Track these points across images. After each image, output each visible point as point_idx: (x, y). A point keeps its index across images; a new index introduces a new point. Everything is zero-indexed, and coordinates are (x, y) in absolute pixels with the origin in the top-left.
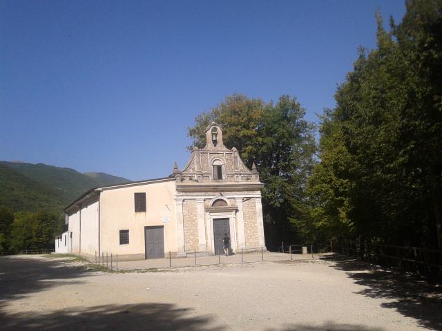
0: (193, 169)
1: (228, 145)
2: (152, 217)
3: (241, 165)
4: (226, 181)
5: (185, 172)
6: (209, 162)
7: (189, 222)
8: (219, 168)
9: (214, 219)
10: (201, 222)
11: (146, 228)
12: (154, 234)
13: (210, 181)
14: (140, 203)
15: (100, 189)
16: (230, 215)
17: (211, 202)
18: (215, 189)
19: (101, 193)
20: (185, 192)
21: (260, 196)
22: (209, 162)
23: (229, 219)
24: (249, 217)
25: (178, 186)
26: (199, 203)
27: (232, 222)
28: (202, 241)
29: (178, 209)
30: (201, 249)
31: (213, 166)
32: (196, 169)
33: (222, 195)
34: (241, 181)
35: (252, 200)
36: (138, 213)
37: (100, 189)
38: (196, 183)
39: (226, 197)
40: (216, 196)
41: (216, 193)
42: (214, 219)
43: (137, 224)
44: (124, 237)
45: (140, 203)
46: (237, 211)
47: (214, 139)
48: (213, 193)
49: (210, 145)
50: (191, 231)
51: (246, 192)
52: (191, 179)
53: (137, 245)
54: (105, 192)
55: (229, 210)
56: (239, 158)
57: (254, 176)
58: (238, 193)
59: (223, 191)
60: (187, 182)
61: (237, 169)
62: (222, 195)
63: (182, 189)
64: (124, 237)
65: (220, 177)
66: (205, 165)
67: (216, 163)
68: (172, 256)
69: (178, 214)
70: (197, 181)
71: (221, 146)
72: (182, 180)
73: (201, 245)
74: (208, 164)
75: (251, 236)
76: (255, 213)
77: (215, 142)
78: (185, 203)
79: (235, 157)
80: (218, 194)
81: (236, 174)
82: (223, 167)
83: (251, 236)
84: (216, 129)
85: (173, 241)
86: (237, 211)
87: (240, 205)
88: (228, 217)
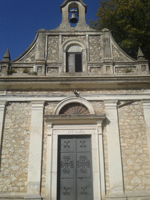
3: (115, 51)
5: (18, 62)
6: (61, 47)
8: (78, 57)
9: (60, 137)
10: (35, 141)
13: (60, 72)
16: (93, 130)
17: (53, 109)
18: (65, 85)
20: (13, 90)
22: (61, 47)
23: (89, 136)
28: (33, 176)
31: (68, 54)
32: (37, 58)
33: (77, 95)
35: (136, 106)
40: (68, 98)
41: (67, 93)
42: (60, 137)
46: (105, 122)
47: (73, 16)
48: (61, 93)
49: (65, 26)
50: (15, 157)
51: (125, 92)
52: (25, 72)
55: (91, 120)
56: (112, 42)
57: (139, 67)
58: (108, 92)
59: (81, 90)
65: (79, 68)
66: (54, 51)
67: (72, 49)
71: (82, 26)
72: (10, 73)
73: (30, 183)
74: (58, 50)
75: (136, 172)
77: (74, 21)
78: (9, 108)
79: (105, 40)
80: (71, 93)
81: (107, 63)
82: (84, 54)
83: (136, 172)
84: (76, 7)
86: (105, 122)
87: (112, 113)
88: (87, 132)
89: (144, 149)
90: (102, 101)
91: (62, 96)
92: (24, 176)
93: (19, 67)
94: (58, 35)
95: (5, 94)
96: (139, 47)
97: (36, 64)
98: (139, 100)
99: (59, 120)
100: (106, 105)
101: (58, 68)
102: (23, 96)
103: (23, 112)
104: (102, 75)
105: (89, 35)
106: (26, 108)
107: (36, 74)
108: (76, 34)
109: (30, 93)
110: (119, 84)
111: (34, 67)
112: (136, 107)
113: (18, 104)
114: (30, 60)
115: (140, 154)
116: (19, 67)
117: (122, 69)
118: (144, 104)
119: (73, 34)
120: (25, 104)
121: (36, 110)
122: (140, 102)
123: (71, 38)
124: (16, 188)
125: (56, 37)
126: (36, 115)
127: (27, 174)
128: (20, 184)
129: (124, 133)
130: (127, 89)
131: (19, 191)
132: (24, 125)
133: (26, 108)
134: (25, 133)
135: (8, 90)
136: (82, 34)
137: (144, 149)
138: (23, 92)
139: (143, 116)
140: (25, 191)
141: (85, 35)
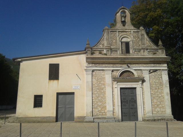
0: (103, 45)
1: (137, 24)
2: (63, 84)
3: (147, 42)
4: (133, 54)
5: (95, 47)
6: (118, 38)
7: (97, 90)
8: (127, 44)
9: (121, 88)
10: (108, 91)
11: (58, 94)
12: (65, 99)
13: (118, 55)
14: (54, 73)
15: (20, 60)
16: (137, 85)
17: (117, 74)
18: (122, 62)
19: (21, 63)
20: (95, 64)
21: (166, 68)
22: (118, 38)
23: (135, 88)
24: (155, 88)
25: (87, 58)
27: (139, 92)
28: (109, 107)
29: (87, 78)
30: (109, 115)
31: (122, 42)
32: (105, 45)
33: (129, 67)
34: (147, 55)
35: (158, 73)
36: (52, 81)
37: (20, 60)
38: (105, 56)
39: (133, 68)
40: (124, 68)
41: (123, 66)
42: (121, 88)
43: (50, 90)
44: (38, 101)
45: (54, 73)
46: (143, 81)
47: (123, 19)
48: (120, 65)
49: (119, 25)
50: (99, 98)
51: (153, 65)
52: (100, 53)
53: (49, 109)
54: (23, 62)
55: (136, 80)
56: (146, 36)
57: (160, 51)
58: (145, 65)
59: (130, 64)
60: (97, 55)
61: (143, 44)
62: (129, 67)
63: (91, 61)
64: (38, 101)
65: (128, 51)
66: (114, 41)
67: (124, 40)
68: (82, 120)
69: (87, 82)
70: (106, 54)
71: (129, 26)
72: (92, 54)
73: (108, 111)
75: (158, 105)
76: (161, 84)
77: (124, 23)
78: (94, 73)
79: (142, 35)
80: (125, 66)
81: (144, 49)
82: (131, 43)
83: (158, 105)
84: (125, 12)
85: (82, 107)
86: (143, 81)
88: (134, 86)
89: (162, 94)
90: (141, 70)
91: (121, 67)
92: (105, 107)
93: (96, 50)
94: (116, 31)
95: (91, 66)
96: (160, 40)
97: (106, 49)
98: (160, 70)
99: (121, 80)
100: (143, 72)
101: (117, 51)
102: (101, 67)
103: (101, 75)
104: (141, 56)
105: (133, 32)
106: (103, 74)
107: (106, 54)
108: (126, 31)
109: (104, 65)
110: (150, 61)
111: (105, 50)
112: (159, 73)
113: (98, 71)
114: (102, 46)
115: (160, 97)
116: (96, 50)
117: (151, 52)
118: (162, 72)
119: (124, 31)
120: (102, 71)
121: (107, 74)
122: (160, 71)
123: (123, 33)
124: (101, 113)
125: (115, 32)
126: (108, 77)
127: (106, 106)
128: (103, 111)
129: (152, 87)
130: (154, 64)
131: (102, 115)
132: (102, 82)
133: (103, 74)
134: (103, 86)
135: (92, 64)
136: (130, 31)
137: (162, 94)
138: (100, 65)
139: (162, 78)
140: (106, 115)
141: (131, 32)
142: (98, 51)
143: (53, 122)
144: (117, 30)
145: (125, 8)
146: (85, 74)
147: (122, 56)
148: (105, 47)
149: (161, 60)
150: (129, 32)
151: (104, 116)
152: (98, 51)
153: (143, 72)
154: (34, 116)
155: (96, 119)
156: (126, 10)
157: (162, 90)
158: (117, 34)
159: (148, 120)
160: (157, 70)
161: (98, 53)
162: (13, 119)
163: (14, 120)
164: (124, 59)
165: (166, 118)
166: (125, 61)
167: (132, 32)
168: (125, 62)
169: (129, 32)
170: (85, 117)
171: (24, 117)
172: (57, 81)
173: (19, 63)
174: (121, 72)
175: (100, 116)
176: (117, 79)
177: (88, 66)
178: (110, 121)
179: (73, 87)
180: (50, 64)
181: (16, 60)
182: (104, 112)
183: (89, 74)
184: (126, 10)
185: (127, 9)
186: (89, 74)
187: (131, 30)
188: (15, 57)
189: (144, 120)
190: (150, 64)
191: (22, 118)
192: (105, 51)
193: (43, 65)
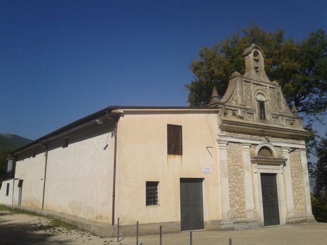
0: (236, 101)
1: (271, 76)
2: (191, 163)
4: (271, 122)
6: (253, 94)
7: (234, 174)
9: (262, 174)
11: (183, 180)
12: (191, 189)
13: (254, 119)
14: (175, 142)
15: (121, 111)
19: (121, 118)
21: (304, 147)
23: (275, 174)
24: (295, 176)
25: (224, 122)
26: (246, 148)
27: (280, 180)
28: (249, 205)
29: (221, 154)
30: (249, 217)
33: (269, 141)
34: (283, 124)
35: (297, 152)
36: (172, 156)
37: (121, 111)
38: (241, 121)
39: (274, 143)
42: (262, 174)
43: (170, 173)
44: (152, 192)
45: (175, 142)
50: (237, 190)
51: (292, 141)
52: (234, 114)
53: (169, 208)
54: (126, 116)
58: (284, 140)
60: (230, 117)
61: (281, 109)
62: (269, 141)
63: (228, 127)
64: (152, 192)
65: (262, 116)
66: (249, 97)
67: (260, 98)
68: (218, 226)
69: (222, 162)
70: (241, 118)
74: (251, 97)
76: (301, 169)
81: (282, 115)
85: (215, 206)
87: (286, 155)
88: (275, 172)
89: (302, 185)
90: (280, 147)
91: (260, 140)
92: (243, 204)
93: (229, 109)
94: (250, 82)
95: (225, 134)
97: (241, 108)
98: (298, 149)
99: (262, 161)
100: (283, 150)
101: (253, 114)
102: (237, 138)
103: (237, 152)
104: (280, 125)
105: (270, 87)
106: (238, 149)
107: (241, 118)
108: (262, 84)
109: (240, 135)
110: (291, 135)
111: (239, 111)
112: (297, 153)
113: (233, 144)
114: (235, 103)
115: (299, 188)
116: (229, 109)
117: (288, 121)
118: (302, 152)
119: (259, 83)
120: (237, 145)
121: (246, 151)
122: (298, 150)
123: (259, 87)
124: (239, 215)
125: (249, 83)
126: (246, 154)
127: (244, 203)
128: (242, 211)
130: (293, 139)
131: (241, 217)
132: (239, 163)
133: (238, 149)
134: (240, 170)
135: (226, 131)
136: (265, 84)
137: (302, 185)
138: (236, 134)
139: (300, 160)
140: (245, 217)
141: (266, 86)
142: (231, 110)
143: (178, 232)
144: (252, 81)
145: (259, 47)
146: (218, 147)
147: (260, 122)
148: (239, 104)
149: (301, 135)
150: (264, 86)
151: (244, 219)
152: (231, 110)
153: (283, 150)
154: (148, 223)
155: (240, 223)
156: (259, 52)
157: (302, 178)
158: (252, 87)
159: (292, 223)
160: (295, 149)
161: (231, 114)
162: (113, 229)
163: (113, 232)
164: (265, 128)
165: (308, 219)
166: (264, 131)
167: (268, 87)
168: (265, 133)
169: (264, 86)
170: (221, 221)
171: (131, 224)
172: (179, 156)
173: (117, 117)
174: (261, 147)
175: (239, 219)
176: (259, 160)
177: (221, 134)
178: (253, 226)
179: (203, 170)
180: (181, 127)
181: (114, 111)
182: (243, 213)
183: (223, 149)
184: (259, 52)
185: (261, 49)
186: (223, 149)
187: (267, 83)
188: (113, 104)
189: (288, 223)
190: (289, 138)
191: (128, 226)
192: (239, 113)
193: (159, 123)
